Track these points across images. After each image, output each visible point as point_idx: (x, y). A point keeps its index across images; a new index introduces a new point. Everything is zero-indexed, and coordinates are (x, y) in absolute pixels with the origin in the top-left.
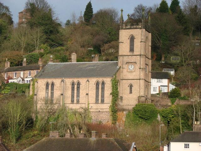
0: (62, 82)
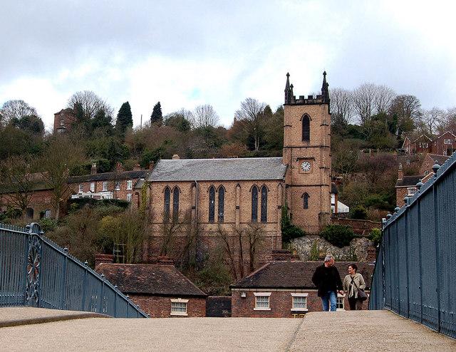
0: (194, 188)
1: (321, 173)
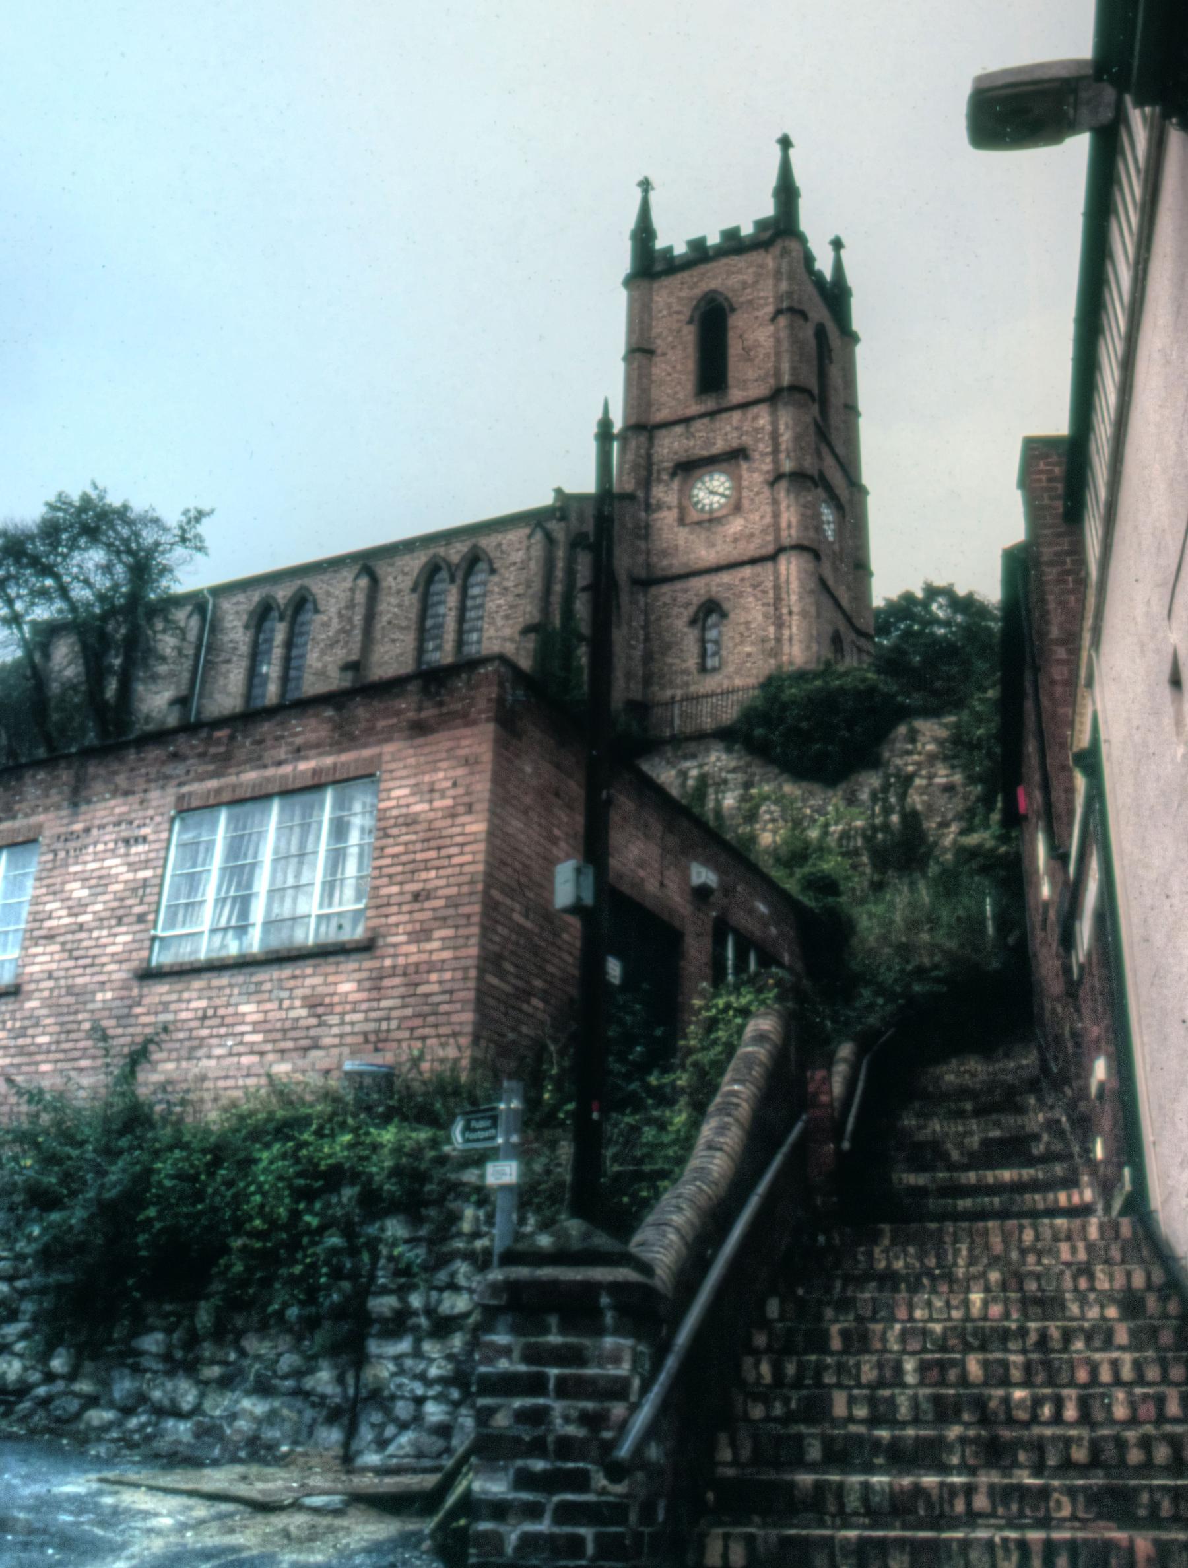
1: (775, 502)
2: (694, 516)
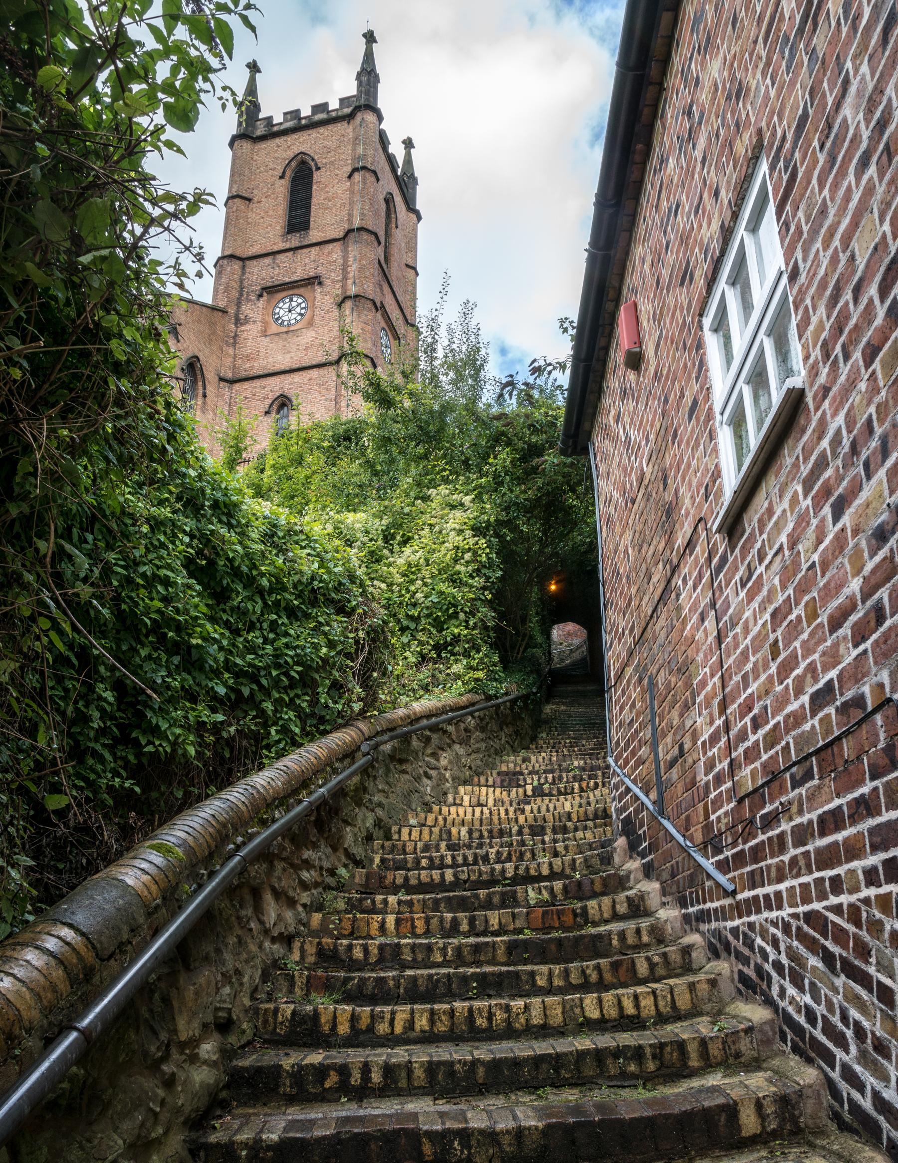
1: (342, 317)
2: (274, 328)
